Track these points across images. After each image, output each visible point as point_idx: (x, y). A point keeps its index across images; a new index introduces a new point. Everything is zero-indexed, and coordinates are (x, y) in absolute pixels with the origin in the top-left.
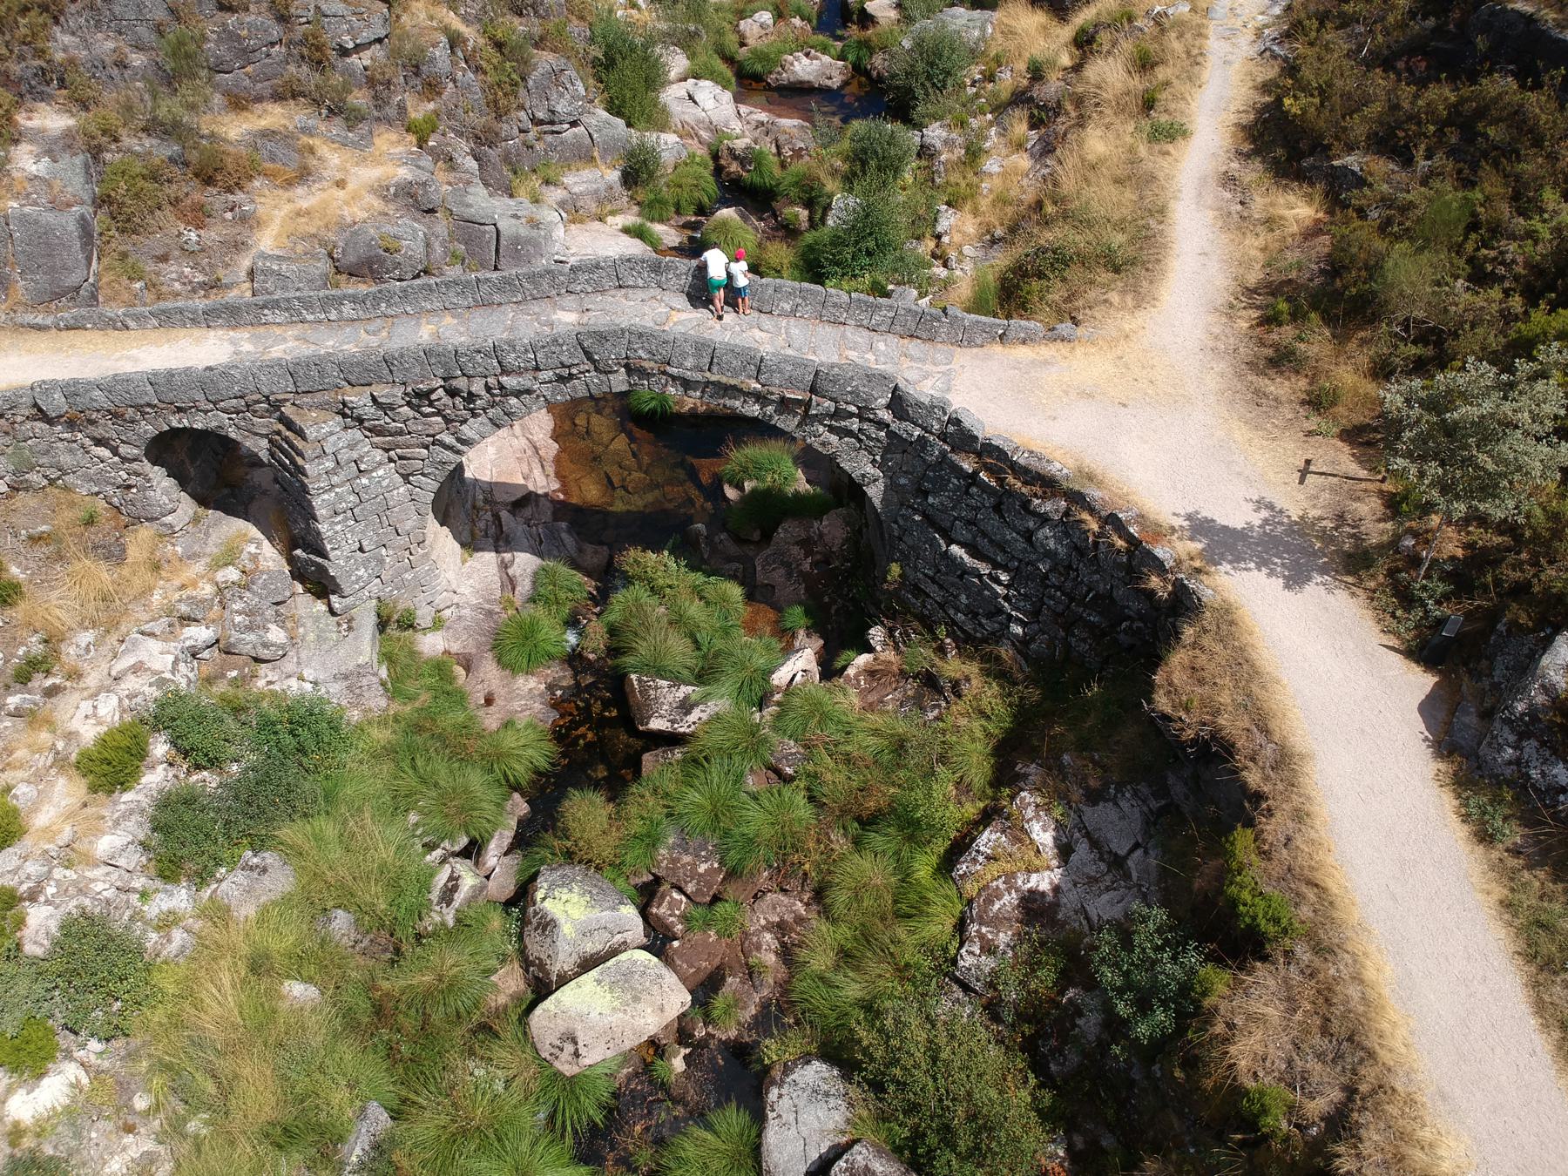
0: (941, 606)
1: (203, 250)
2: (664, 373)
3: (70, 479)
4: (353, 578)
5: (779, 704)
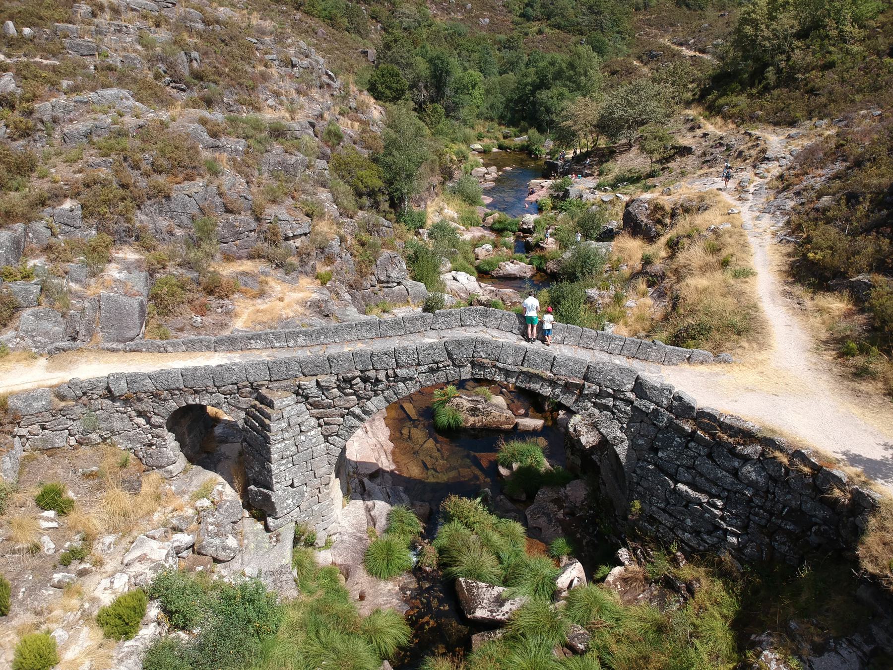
0: (672, 530)
1: (203, 327)
2: (494, 366)
3: (116, 438)
4: (285, 505)
5: (566, 598)
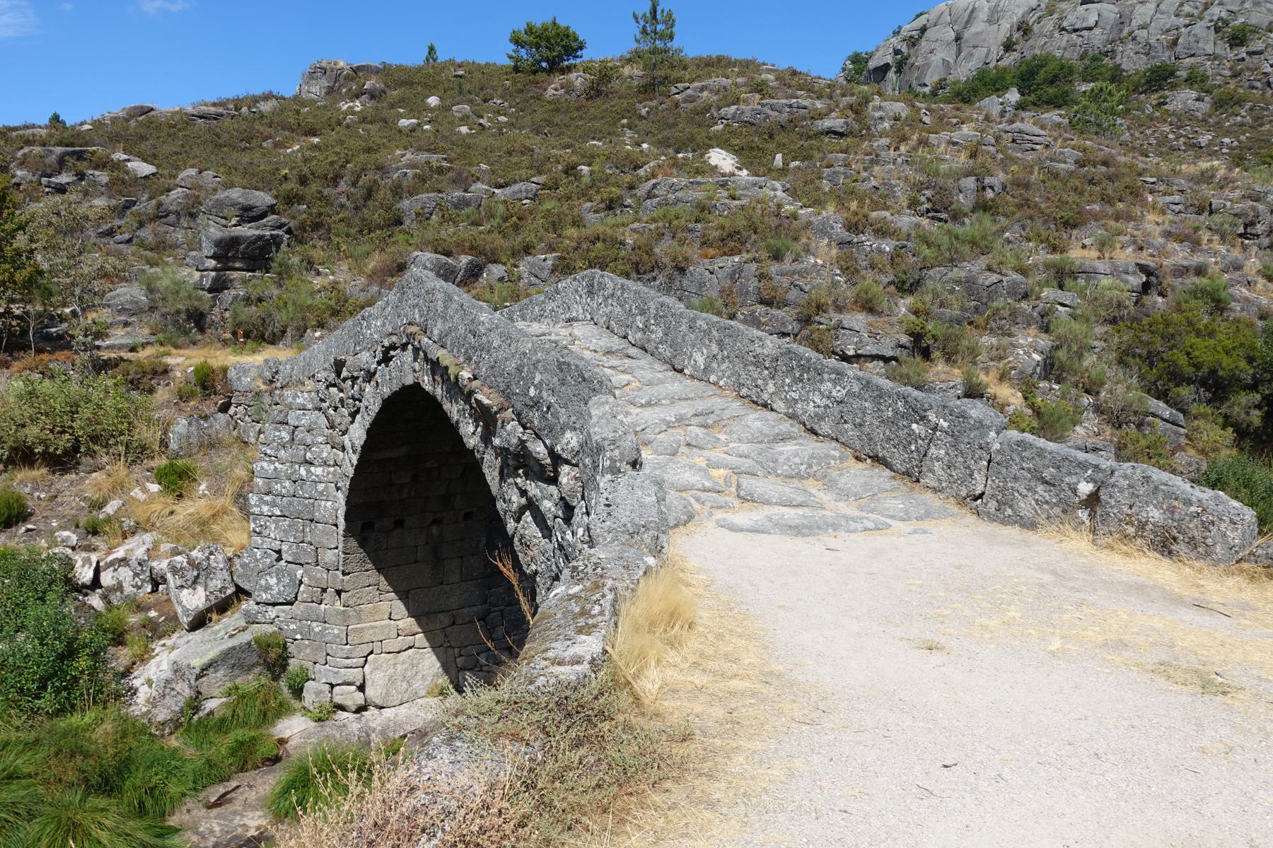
4: (263, 582)
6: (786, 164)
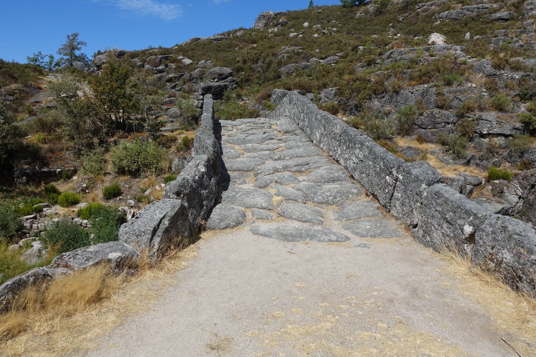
6: (472, 37)
